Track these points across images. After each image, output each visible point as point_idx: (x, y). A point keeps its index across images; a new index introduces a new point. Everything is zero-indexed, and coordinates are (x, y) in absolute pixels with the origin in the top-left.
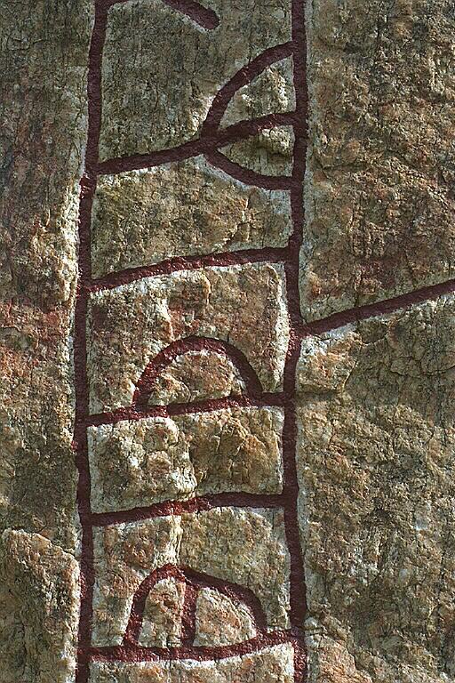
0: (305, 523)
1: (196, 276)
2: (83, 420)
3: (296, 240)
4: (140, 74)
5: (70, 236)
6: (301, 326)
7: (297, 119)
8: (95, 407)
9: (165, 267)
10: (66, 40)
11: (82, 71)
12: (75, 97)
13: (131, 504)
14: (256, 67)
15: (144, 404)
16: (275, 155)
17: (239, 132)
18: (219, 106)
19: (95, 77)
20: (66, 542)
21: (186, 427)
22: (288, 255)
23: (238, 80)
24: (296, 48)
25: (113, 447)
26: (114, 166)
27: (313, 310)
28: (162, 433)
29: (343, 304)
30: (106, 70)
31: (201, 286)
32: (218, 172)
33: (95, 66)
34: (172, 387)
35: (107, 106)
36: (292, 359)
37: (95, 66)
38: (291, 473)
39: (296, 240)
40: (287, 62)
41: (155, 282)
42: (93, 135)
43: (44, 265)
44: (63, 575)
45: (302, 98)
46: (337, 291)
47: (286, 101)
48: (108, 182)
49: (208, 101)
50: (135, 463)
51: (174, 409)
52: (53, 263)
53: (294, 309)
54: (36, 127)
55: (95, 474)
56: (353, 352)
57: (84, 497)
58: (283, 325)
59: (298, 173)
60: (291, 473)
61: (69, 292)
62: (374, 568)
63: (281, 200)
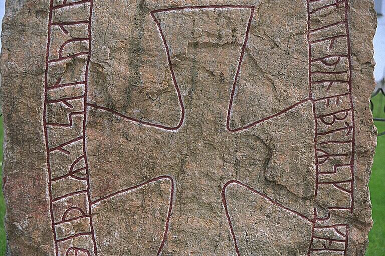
0: (95, 236)
1: (71, 197)
2: (54, 224)
3: (89, 188)
4: (57, 164)
5: (48, 193)
6: (91, 203)
7: (86, 168)
8: (55, 222)
9: (65, 196)
10: (42, 159)
11: (46, 164)
12: (46, 169)
13: (64, 238)
14: (78, 160)
15: (64, 220)
16: (83, 175)
17: (75, 172)
18: (72, 167)
19: (48, 165)
20: (52, 246)
21: (72, 223)
22: (88, 191)
23: (75, 163)
24: (85, 156)
25: (59, 228)
26: (54, 180)
27: (93, 200)
28: (68, 225)
29: (98, 198)
30: (50, 164)
31: (72, 198)
32: (73, 179)
33: (48, 162)
34: (69, 217)
35: (51, 170)
36: (90, 209)
37: (48, 162)
38: (92, 228)
39: (89, 188)
40: (83, 158)
41: (64, 199)
42: (50, 175)
43: (43, 199)
44: (52, 252)
45: (87, 165)
46: (97, 196)
47: (84, 165)
48: (53, 182)
49: (70, 167)
50: (64, 230)
51: (69, 220)
52: (45, 198)
53: (89, 200)
54: (39, 175)
55: (57, 234)
56: (101, 206)
57: (55, 237)
58: (88, 203)
59: (88, 177)
60: (92, 228)
61: (48, 202)
62: (108, 243)
63: (85, 181)
